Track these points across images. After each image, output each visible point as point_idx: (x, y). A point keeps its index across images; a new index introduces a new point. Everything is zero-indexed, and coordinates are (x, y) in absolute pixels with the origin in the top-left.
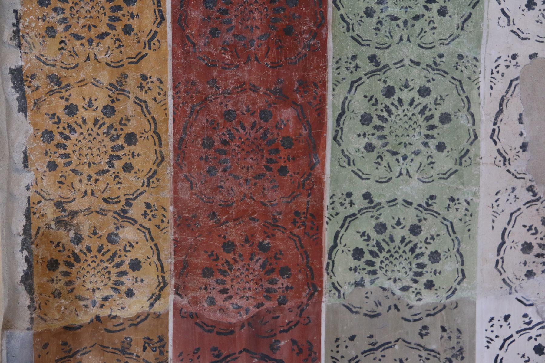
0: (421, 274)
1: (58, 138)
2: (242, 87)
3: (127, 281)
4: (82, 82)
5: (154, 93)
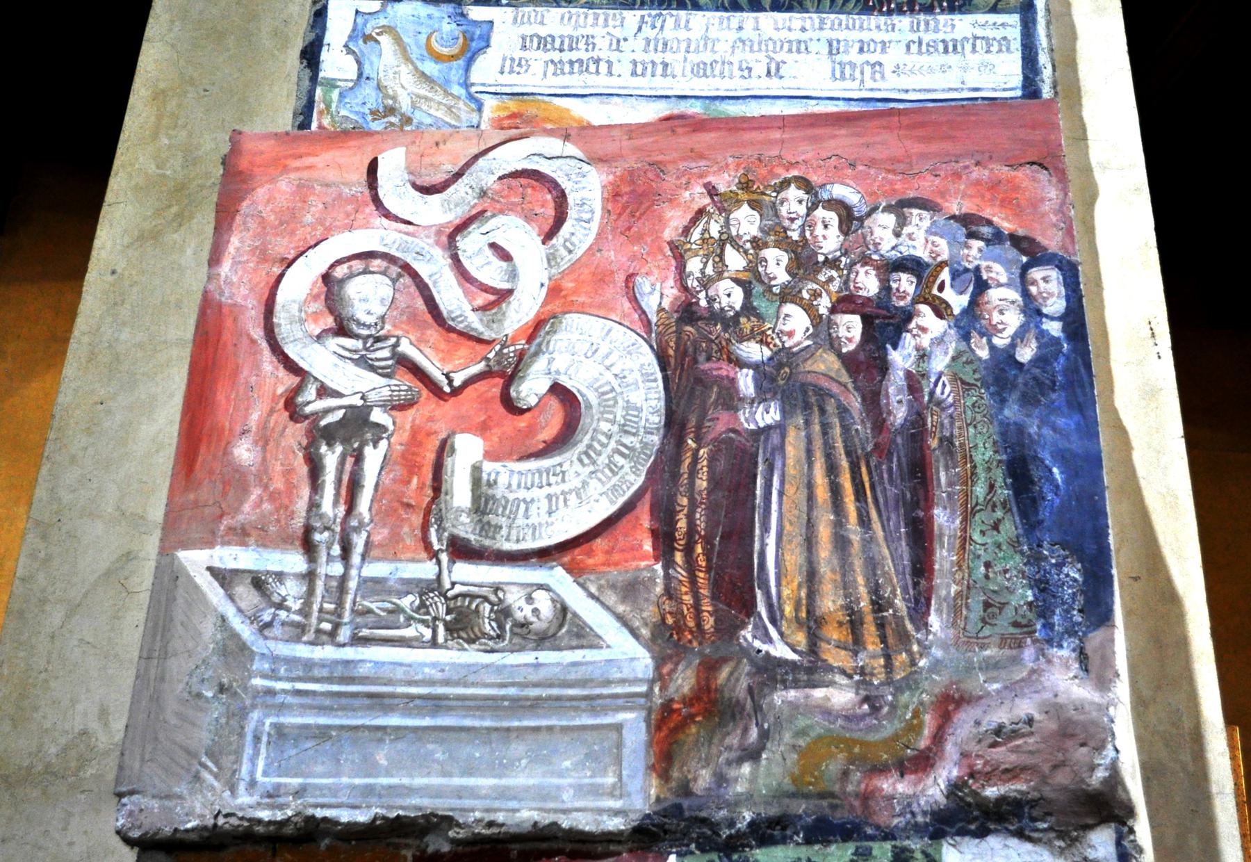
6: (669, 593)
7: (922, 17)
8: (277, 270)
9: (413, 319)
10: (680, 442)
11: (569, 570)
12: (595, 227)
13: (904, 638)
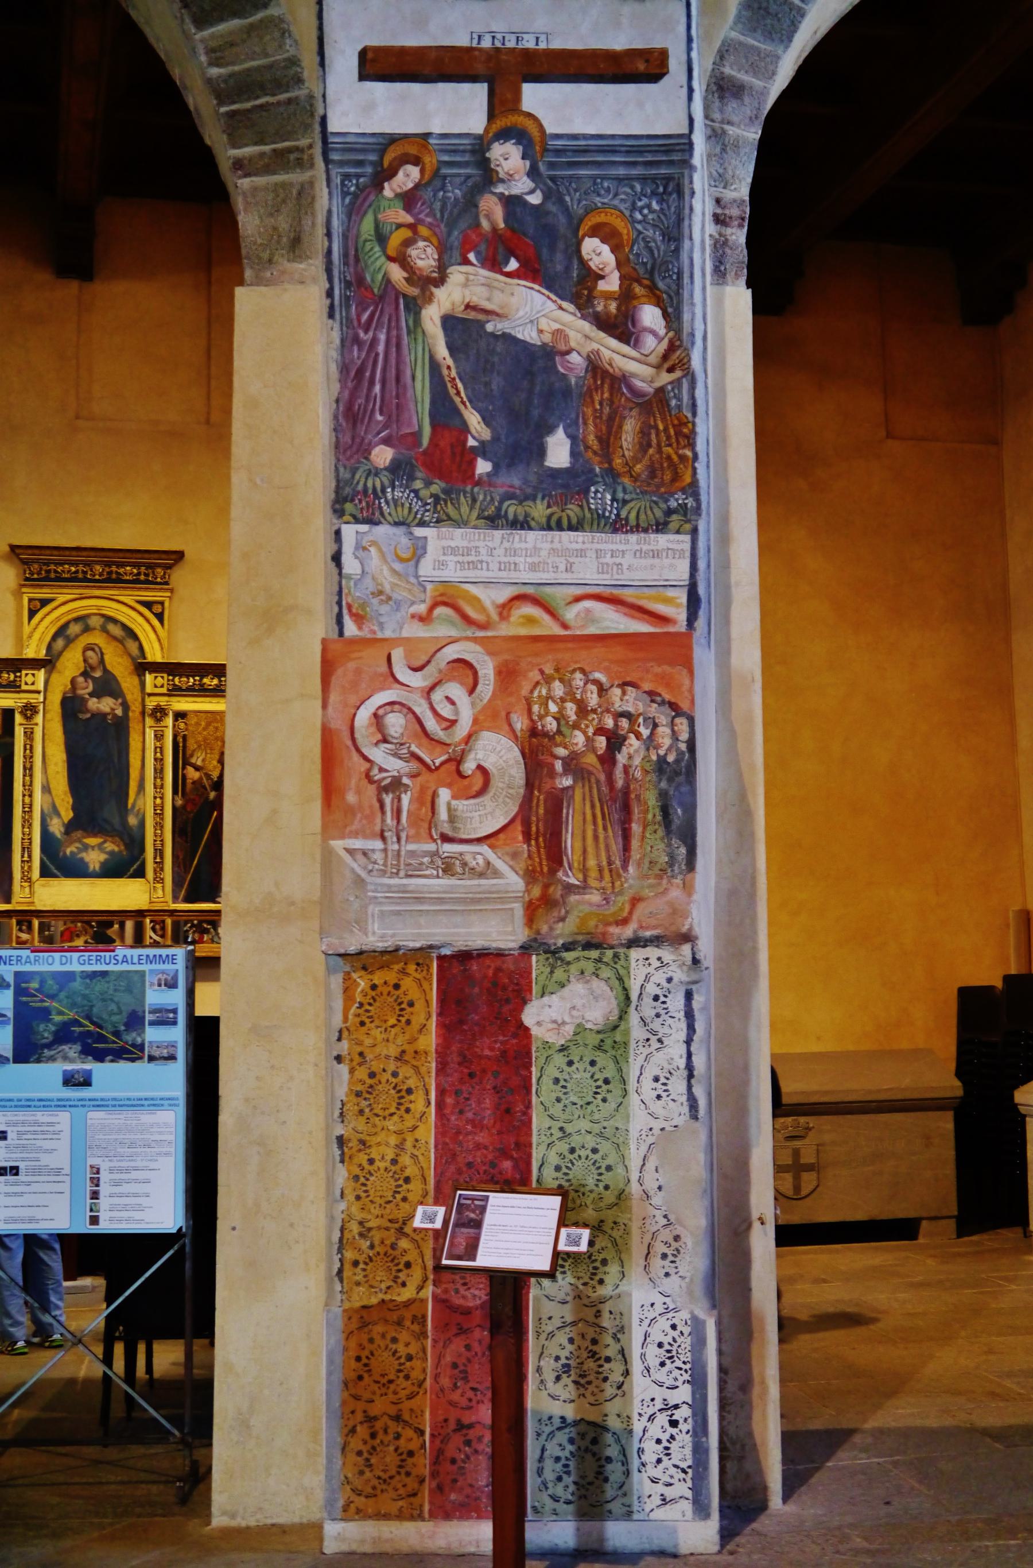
0: (595, 1274)
1: (362, 1180)
2: (478, 1146)
3: (402, 1276)
4: (379, 1144)
5: (422, 1151)
6: (530, 857)
7: (642, 535)
8: (353, 711)
9: (416, 735)
10: (532, 793)
11: (490, 847)
12: (491, 688)
13: (619, 876)
